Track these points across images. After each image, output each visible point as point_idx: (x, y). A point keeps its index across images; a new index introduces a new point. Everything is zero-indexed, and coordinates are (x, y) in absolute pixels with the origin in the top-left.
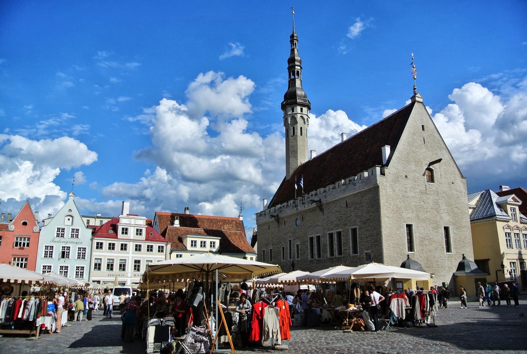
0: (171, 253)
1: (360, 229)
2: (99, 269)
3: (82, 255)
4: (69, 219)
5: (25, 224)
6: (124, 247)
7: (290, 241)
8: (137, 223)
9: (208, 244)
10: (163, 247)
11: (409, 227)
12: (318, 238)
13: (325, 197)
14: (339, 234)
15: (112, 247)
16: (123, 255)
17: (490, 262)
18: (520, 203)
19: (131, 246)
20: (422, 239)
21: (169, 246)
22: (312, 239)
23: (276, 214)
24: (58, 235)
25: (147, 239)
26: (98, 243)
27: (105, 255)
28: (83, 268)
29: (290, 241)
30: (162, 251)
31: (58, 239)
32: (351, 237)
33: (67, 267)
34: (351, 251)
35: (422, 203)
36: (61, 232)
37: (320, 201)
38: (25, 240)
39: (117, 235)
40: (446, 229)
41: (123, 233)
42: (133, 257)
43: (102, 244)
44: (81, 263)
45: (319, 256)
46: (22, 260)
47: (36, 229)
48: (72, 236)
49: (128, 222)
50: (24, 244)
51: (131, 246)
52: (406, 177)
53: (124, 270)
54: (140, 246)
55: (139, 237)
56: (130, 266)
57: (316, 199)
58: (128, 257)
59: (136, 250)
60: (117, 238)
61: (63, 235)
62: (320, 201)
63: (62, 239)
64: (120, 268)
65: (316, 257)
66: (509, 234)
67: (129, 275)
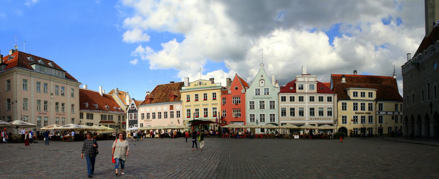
0: (338, 102)
2: (285, 115)
4: (262, 82)
5: (237, 89)
6: (301, 99)
8: (310, 80)
10: (331, 97)
15: (292, 99)
19: (306, 98)
24: (256, 94)
25: (318, 92)
26: (282, 97)
27: (288, 105)
28: (274, 115)
30: (331, 101)
33: (264, 115)
39: (296, 91)
43: (285, 97)
44: (273, 112)
47: (243, 91)
51: (306, 98)
53: (303, 115)
54: (313, 97)
56: (307, 113)
58: (305, 106)
59: (310, 100)
60: (295, 92)
61: (259, 94)
63: (259, 96)
64: (300, 115)
67: (307, 119)
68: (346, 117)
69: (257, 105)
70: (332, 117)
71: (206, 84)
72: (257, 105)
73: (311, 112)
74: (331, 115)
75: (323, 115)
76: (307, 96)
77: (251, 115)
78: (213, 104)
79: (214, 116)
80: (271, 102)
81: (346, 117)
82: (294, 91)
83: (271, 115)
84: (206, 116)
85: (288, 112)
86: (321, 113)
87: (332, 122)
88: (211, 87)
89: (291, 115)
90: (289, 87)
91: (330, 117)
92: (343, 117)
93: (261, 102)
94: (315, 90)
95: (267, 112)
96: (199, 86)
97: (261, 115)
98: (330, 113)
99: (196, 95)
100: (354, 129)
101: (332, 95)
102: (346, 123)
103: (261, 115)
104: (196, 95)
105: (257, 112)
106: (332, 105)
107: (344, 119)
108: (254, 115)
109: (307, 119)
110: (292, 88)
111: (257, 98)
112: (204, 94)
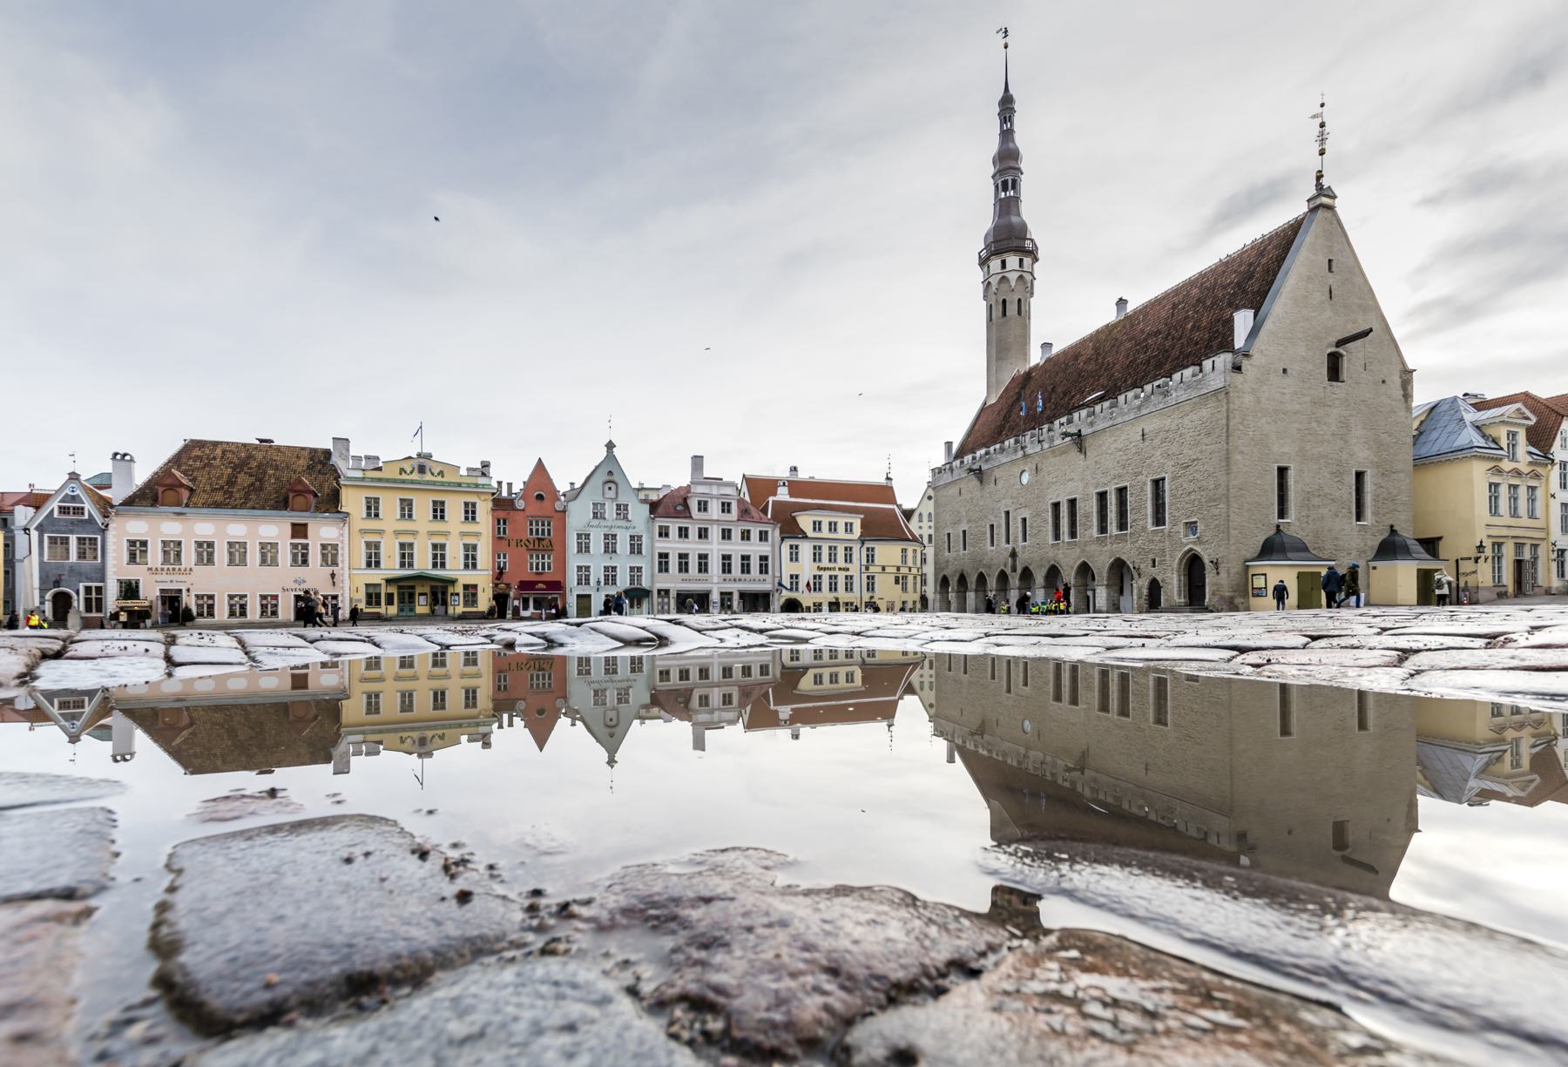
1: (1174, 479)
5: (540, 497)
6: (703, 534)
7: (1007, 513)
9: (841, 527)
11: (1282, 471)
12: (1072, 502)
13: (1092, 424)
14: (1122, 492)
15: (683, 533)
16: (702, 547)
17: (1441, 543)
18: (1531, 423)
19: (715, 533)
20: (1307, 497)
21: (777, 532)
22: (1056, 506)
23: (976, 467)
24: (595, 515)
28: (639, 569)
29: (1007, 513)
31: (596, 522)
32: (1149, 495)
33: (614, 569)
34: (1150, 520)
35: (1314, 425)
37: (1079, 434)
40: (1360, 476)
44: (637, 561)
45: (1073, 534)
51: (715, 533)
52: (1285, 371)
53: (706, 571)
55: (726, 517)
56: (715, 565)
57: (1072, 430)
62: (1079, 434)
63: (603, 523)
65: (1065, 537)
66: (1497, 485)
67: (715, 580)
69: (597, 543)
70: (768, 577)
72: (597, 543)
77: (579, 568)
80: (632, 537)
82: (685, 512)
83: (632, 569)
85: (673, 562)
86: (746, 568)
87: (766, 587)
88: (459, 485)
90: (670, 507)
91: (763, 576)
93: (606, 537)
95: (623, 562)
96: (415, 476)
97: (606, 569)
98: (764, 569)
99: (407, 505)
101: (769, 528)
103: (606, 569)
104: (407, 505)
105: (597, 562)
108: (587, 568)
109: (715, 580)
112: (435, 503)
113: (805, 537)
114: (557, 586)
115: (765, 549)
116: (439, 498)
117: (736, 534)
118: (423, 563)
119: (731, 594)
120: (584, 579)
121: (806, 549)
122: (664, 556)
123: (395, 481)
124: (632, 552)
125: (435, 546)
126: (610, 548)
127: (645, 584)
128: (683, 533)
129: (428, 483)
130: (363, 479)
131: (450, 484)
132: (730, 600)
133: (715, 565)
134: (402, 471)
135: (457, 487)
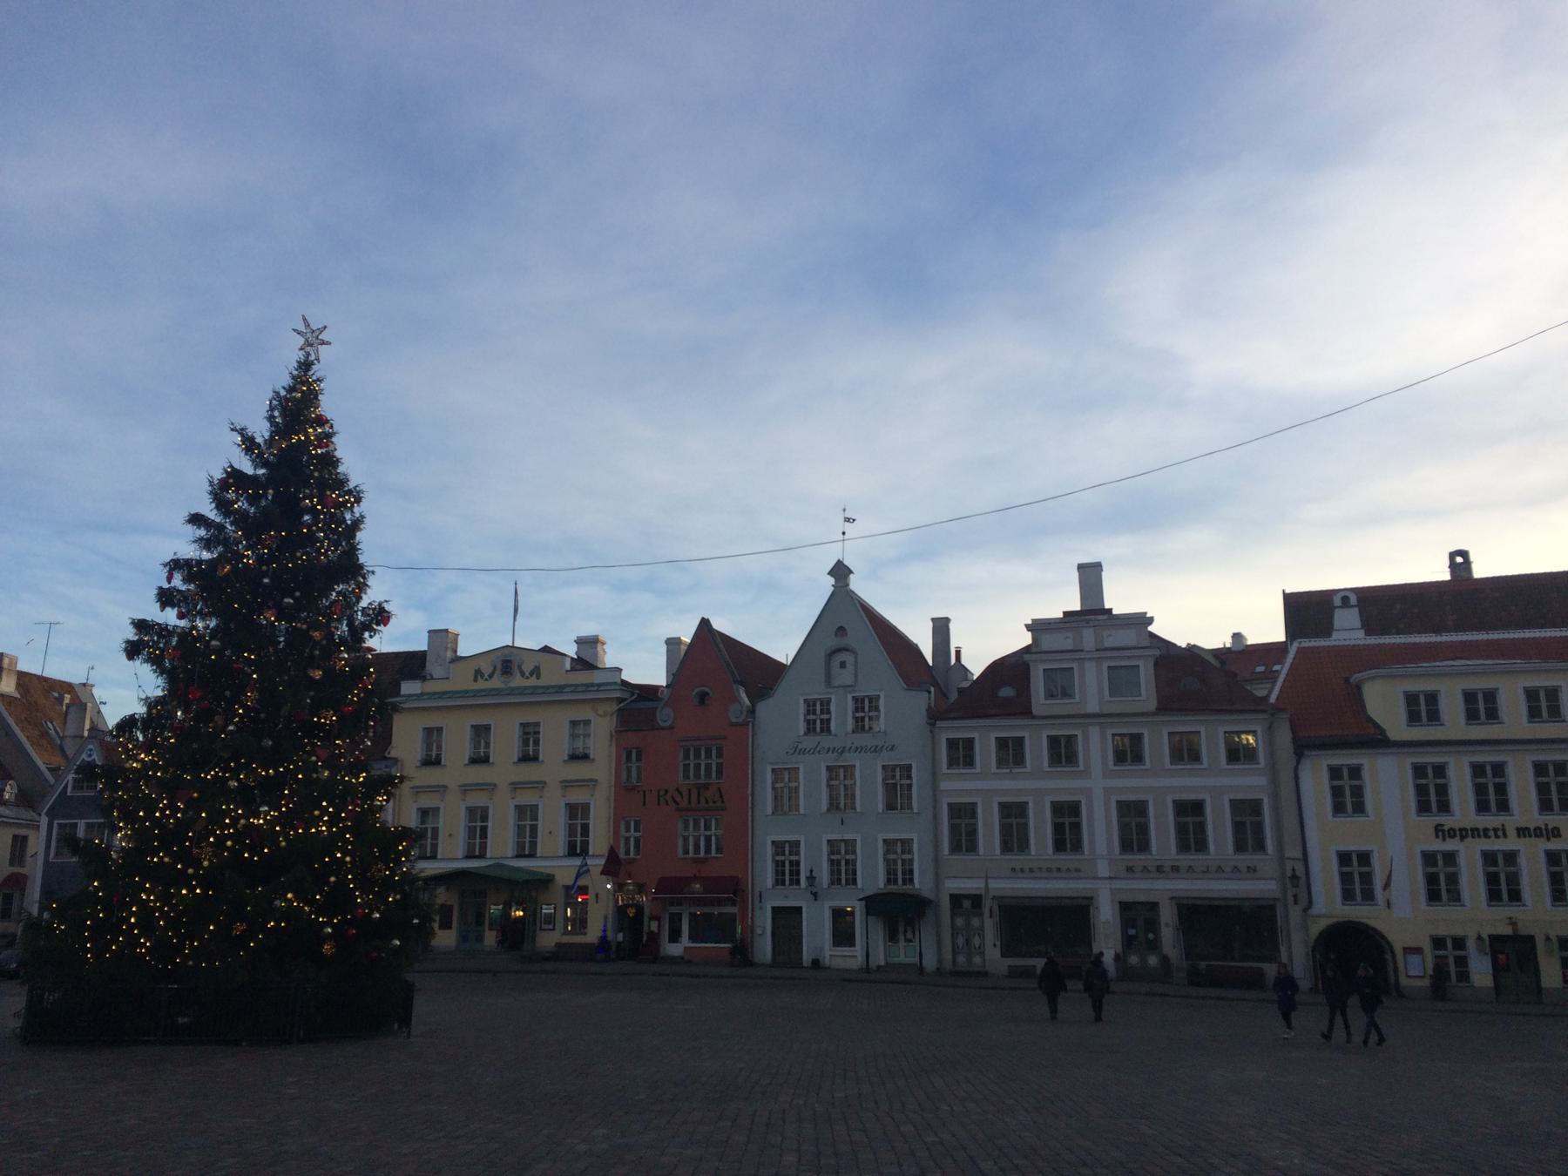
2: (972, 847)
3: (896, 794)
4: (843, 665)
5: (703, 697)
6: (1063, 752)
8: (1108, 644)
15: (1011, 752)
19: (1095, 746)
24: (810, 728)
26: (952, 744)
28: (906, 844)
33: (850, 845)
36: (817, 718)
38: (708, 755)
41: (1050, 695)
42: (1108, 791)
43: (969, 743)
46: (707, 827)
48: (860, 726)
49: (1069, 645)
50: (708, 767)
51: (1095, 746)
53: (1077, 846)
56: (1100, 830)
59: (1120, 757)
60: (1027, 712)
61: (826, 727)
63: (827, 742)
67: (1103, 869)
68: (1365, 858)
71: (536, 672)
73: (1124, 828)
74: (1260, 846)
75: (1202, 846)
76: (1094, 732)
78: (567, 785)
79: (572, 852)
81: (1365, 858)
82: (1021, 708)
84: (526, 849)
87: (1264, 887)
88: (560, 689)
89: (1006, 847)
92: (1344, 858)
94: (1147, 694)
99: (481, 731)
100: (1438, 942)
102: (1368, 896)
104: (481, 731)
106: (1261, 781)
107: (1356, 872)
109: (1103, 869)
110: (1007, 692)
111: (812, 751)
113: (1377, 740)
114: (734, 889)
115: (1250, 782)
116: (530, 716)
117: (1156, 743)
118: (501, 846)
119: (1154, 906)
120: (787, 872)
121: (1388, 780)
122: (963, 814)
123: (464, 694)
124: (890, 807)
125: (520, 810)
126: (840, 802)
127: (922, 883)
128: (1011, 752)
129: (513, 691)
130: (420, 696)
131: (546, 689)
132: (1152, 925)
133: (1100, 830)
134: (478, 674)
135: (557, 696)
